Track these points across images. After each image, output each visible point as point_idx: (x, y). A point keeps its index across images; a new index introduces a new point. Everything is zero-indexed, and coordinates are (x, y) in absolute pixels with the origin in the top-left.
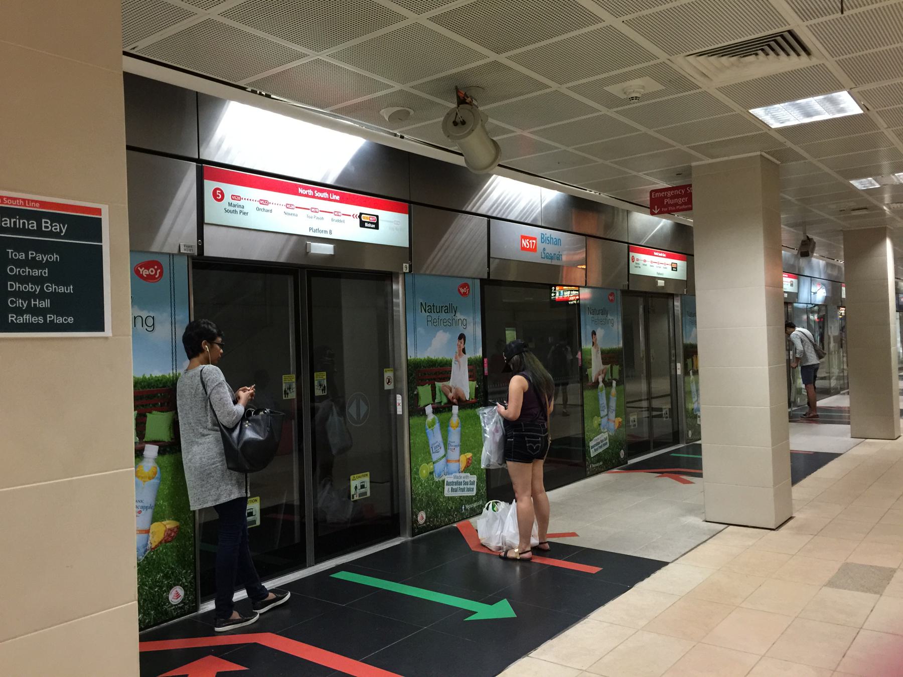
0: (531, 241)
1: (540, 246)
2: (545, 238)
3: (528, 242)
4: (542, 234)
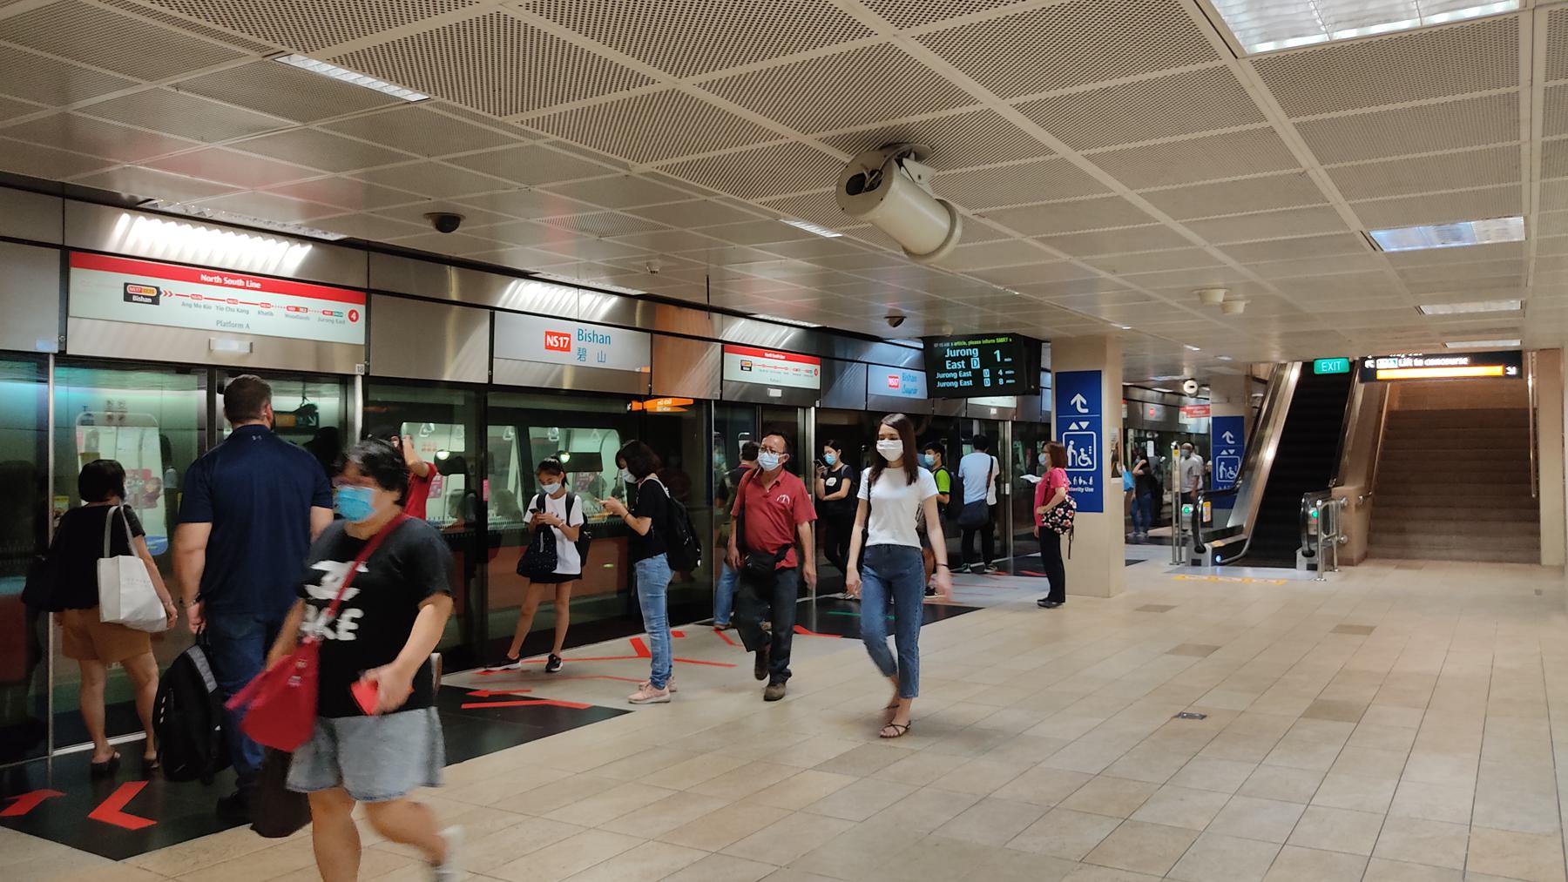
0: (561, 339)
1: (575, 344)
3: (557, 339)
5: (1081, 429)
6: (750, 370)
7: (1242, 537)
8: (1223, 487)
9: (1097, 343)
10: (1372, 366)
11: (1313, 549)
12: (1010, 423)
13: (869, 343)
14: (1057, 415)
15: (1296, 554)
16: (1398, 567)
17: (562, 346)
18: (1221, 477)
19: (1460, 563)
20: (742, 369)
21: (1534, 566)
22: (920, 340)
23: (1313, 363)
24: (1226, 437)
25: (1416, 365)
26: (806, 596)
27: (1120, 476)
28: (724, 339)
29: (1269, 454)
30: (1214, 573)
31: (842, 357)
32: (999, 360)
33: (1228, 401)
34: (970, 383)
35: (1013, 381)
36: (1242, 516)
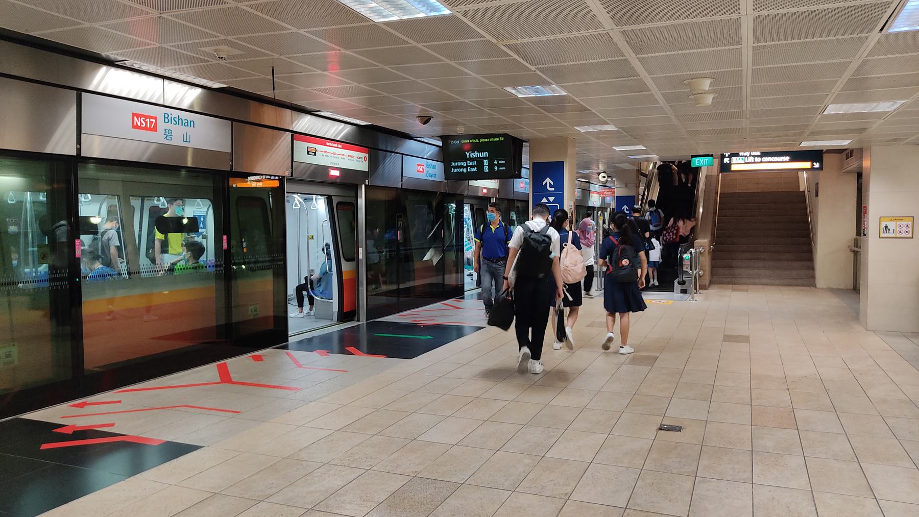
0: (148, 120)
1: (161, 126)
2: (169, 118)
4: (165, 114)
5: (549, 202)
6: (315, 155)
9: (561, 142)
10: (728, 162)
11: (684, 279)
12: (494, 199)
15: (674, 283)
16: (733, 290)
17: (148, 126)
20: (308, 154)
21: (813, 288)
22: (439, 138)
23: (689, 162)
24: (624, 209)
25: (756, 161)
28: (294, 130)
31: (384, 149)
33: (626, 186)
34: (475, 169)
35: (505, 168)
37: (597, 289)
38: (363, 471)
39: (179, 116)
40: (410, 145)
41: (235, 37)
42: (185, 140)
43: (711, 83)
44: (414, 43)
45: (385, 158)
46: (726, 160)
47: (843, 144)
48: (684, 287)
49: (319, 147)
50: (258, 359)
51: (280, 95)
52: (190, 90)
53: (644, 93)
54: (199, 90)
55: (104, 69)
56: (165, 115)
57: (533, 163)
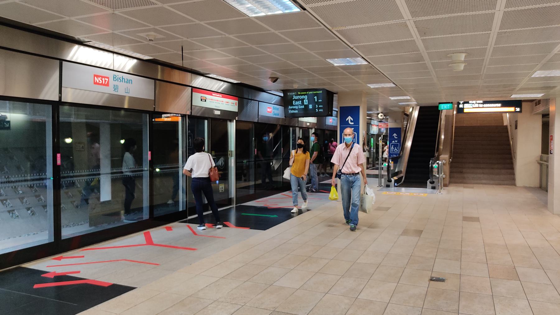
0: (103, 79)
1: (112, 83)
2: (117, 78)
4: (114, 75)
6: (205, 101)
7: (401, 175)
8: (392, 155)
9: (359, 94)
10: (462, 107)
11: (434, 180)
12: (314, 129)
13: (260, 92)
14: (340, 125)
15: (427, 182)
16: (464, 187)
17: (104, 83)
18: (392, 151)
19: (484, 185)
20: (201, 100)
21: (514, 186)
22: (282, 91)
23: (437, 107)
25: (480, 107)
26: (231, 205)
27: (365, 152)
28: (193, 86)
29: (409, 144)
30: (395, 191)
31: (247, 98)
32: (316, 101)
33: (395, 122)
36: (403, 166)
37: (378, 185)
38: (240, 306)
39: (122, 77)
40: (263, 96)
41: (160, 26)
42: (126, 92)
43: (465, 56)
44: (273, 31)
45: (247, 104)
46: (461, 106)
47: (539, 96)
48: (433, 185)
49: (208, 97)
50: (169, 229)
51: (186, 65)
52: (130, 61)
53: (420, 62)
54: (135, 61)
55: (76, 47)
56: (114, 76)
57: (340, 107)
